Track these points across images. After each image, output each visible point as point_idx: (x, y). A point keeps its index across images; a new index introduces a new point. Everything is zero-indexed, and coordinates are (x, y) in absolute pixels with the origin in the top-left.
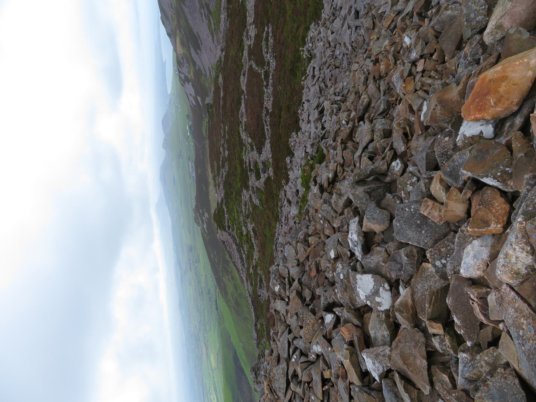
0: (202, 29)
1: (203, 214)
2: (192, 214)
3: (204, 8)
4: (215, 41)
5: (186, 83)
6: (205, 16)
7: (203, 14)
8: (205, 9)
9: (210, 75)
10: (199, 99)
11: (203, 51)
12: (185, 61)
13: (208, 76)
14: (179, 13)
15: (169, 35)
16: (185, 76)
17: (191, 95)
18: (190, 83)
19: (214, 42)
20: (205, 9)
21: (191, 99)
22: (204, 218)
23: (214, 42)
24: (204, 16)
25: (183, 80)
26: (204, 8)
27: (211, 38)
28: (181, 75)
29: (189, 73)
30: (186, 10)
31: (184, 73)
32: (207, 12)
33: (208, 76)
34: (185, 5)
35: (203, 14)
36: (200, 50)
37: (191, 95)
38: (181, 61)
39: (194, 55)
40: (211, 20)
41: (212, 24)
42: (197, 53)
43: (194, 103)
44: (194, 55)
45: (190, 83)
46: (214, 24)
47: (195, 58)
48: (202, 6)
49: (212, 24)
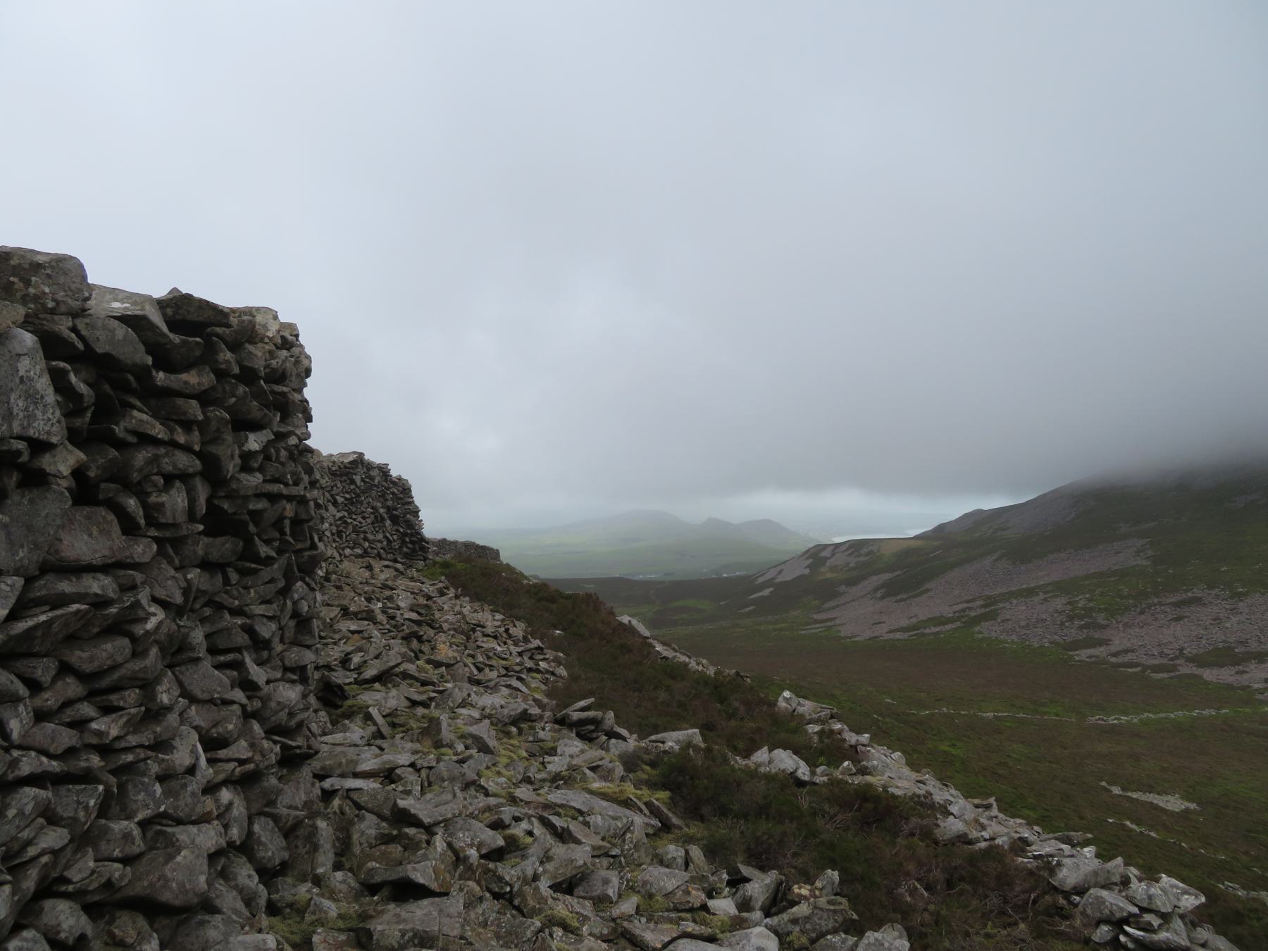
0: (936, 604)
4: (891, 636)
5: (810, 561)
6: (963, 610)
7: (970, 605)
8: (983, 610)
9: (817, 621)
10: (766, 592)
12: (863, 559)
13: (815, 616)
16: (826, 558)
17: (780, 572)
18: (807, 571)
19: (891, 631)
20: (983, 610)
23: (891, 631)
24: (965, 605)
25: (817, 555)
27: (904, 623)
28: (830, 549)
29: (834, 569)
30: (987, 562)
31: (833, 555)
32: (973, 614)
33: (815, 616)
34: (1000, 558)
35: (970, 605)
36: (882, 598)
37: (780, 572)
39: (875, 580)
40: (949, 627)
41: (938, 629)
42: (876, 590)
43: (761, 580)
44: (875, 580)
45: (807, 571)
46: (938, 633)
47: (866, 583)
48: (991, 601)
49: (938, 629)
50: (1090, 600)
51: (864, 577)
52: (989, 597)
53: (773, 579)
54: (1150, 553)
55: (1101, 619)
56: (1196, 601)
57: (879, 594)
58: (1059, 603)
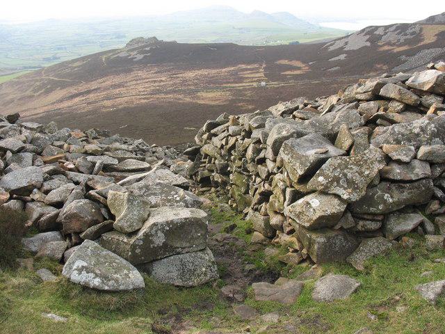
1: (141, 53)
2: (147, 35)
5: (368, 37)
10: (342, 57)
12: (408, 37)
16: (380, 37)
17: (346, 43)
18: (368, 44)
22: (135, 53)
25: (371, 32)
29: (389, 44)
31: (386, 33)
37: (346, 43)
38: (408, 32)
43: (332, 48)
45: (368, 44)
53: (342, 48)
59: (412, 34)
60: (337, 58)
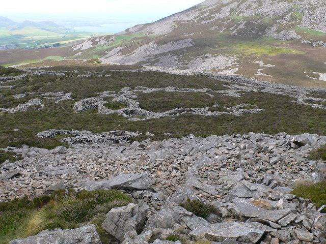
3: (154, 58)
5: (92, 42)
11: (121, 57)
14: (147, 40)
15: (127, 30)
16: (97, 43)
18: (92, 46)
21: (79, 47)
26: (154, 58)
30: (150, 44)
39: (116, 50)
42: (118, 52)
43: (75, 49)
44: (116, 50)
45: (92, 46)
48: (156, 56)
50: (183, 57)
51: (113, 48)
52: (154, 56)
53: (80, 49)
54: (194, 43)
55: (186, 61)
56: (207, 57)
57: (120, 53)
58: (175, 57)
59: (111, 40)
60: (77, 54)
